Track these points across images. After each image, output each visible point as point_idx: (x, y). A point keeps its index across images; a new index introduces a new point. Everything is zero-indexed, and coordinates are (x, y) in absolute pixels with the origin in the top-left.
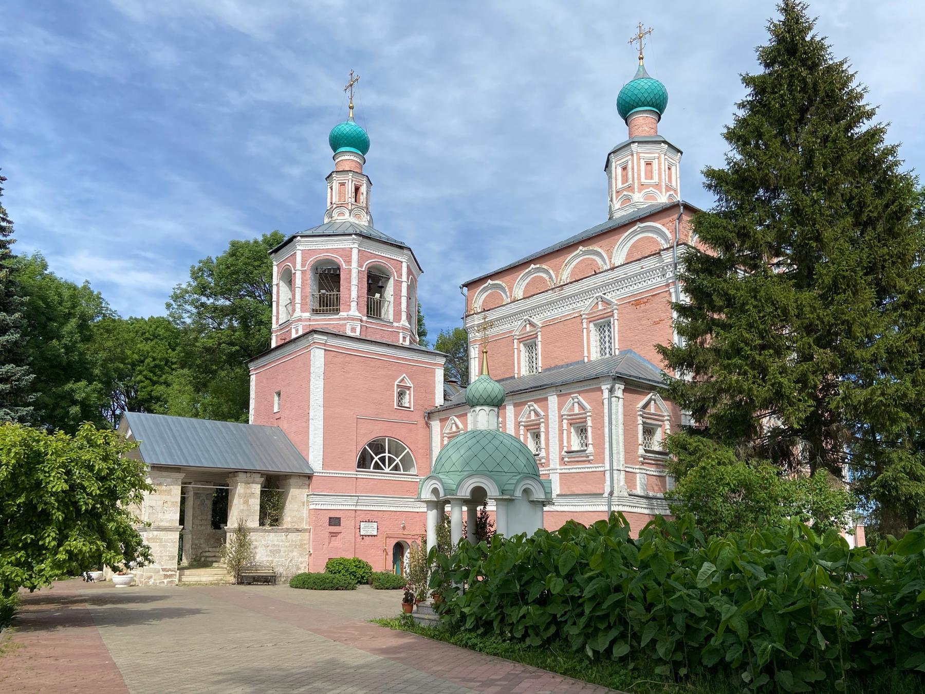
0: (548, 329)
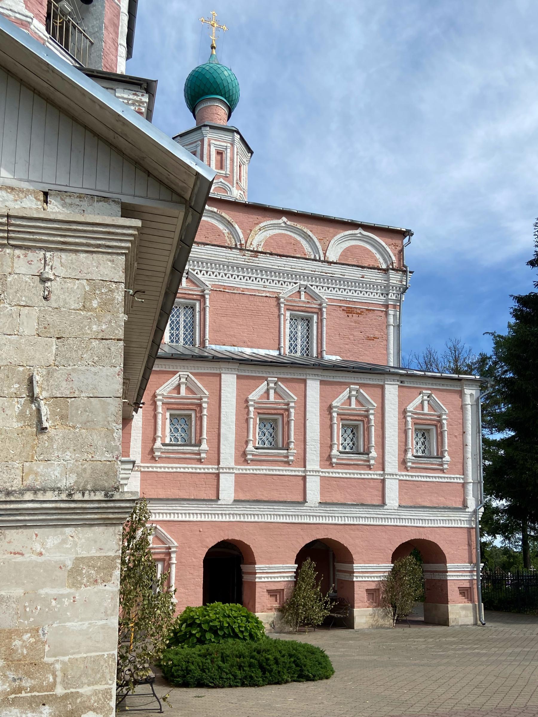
0: (221, 295)
